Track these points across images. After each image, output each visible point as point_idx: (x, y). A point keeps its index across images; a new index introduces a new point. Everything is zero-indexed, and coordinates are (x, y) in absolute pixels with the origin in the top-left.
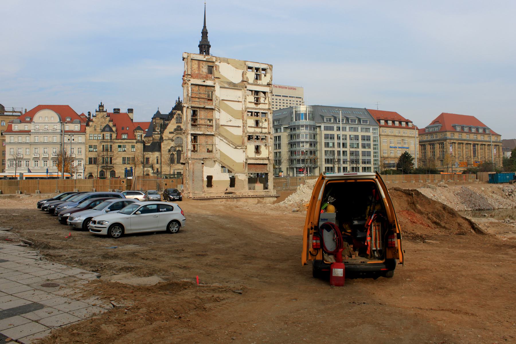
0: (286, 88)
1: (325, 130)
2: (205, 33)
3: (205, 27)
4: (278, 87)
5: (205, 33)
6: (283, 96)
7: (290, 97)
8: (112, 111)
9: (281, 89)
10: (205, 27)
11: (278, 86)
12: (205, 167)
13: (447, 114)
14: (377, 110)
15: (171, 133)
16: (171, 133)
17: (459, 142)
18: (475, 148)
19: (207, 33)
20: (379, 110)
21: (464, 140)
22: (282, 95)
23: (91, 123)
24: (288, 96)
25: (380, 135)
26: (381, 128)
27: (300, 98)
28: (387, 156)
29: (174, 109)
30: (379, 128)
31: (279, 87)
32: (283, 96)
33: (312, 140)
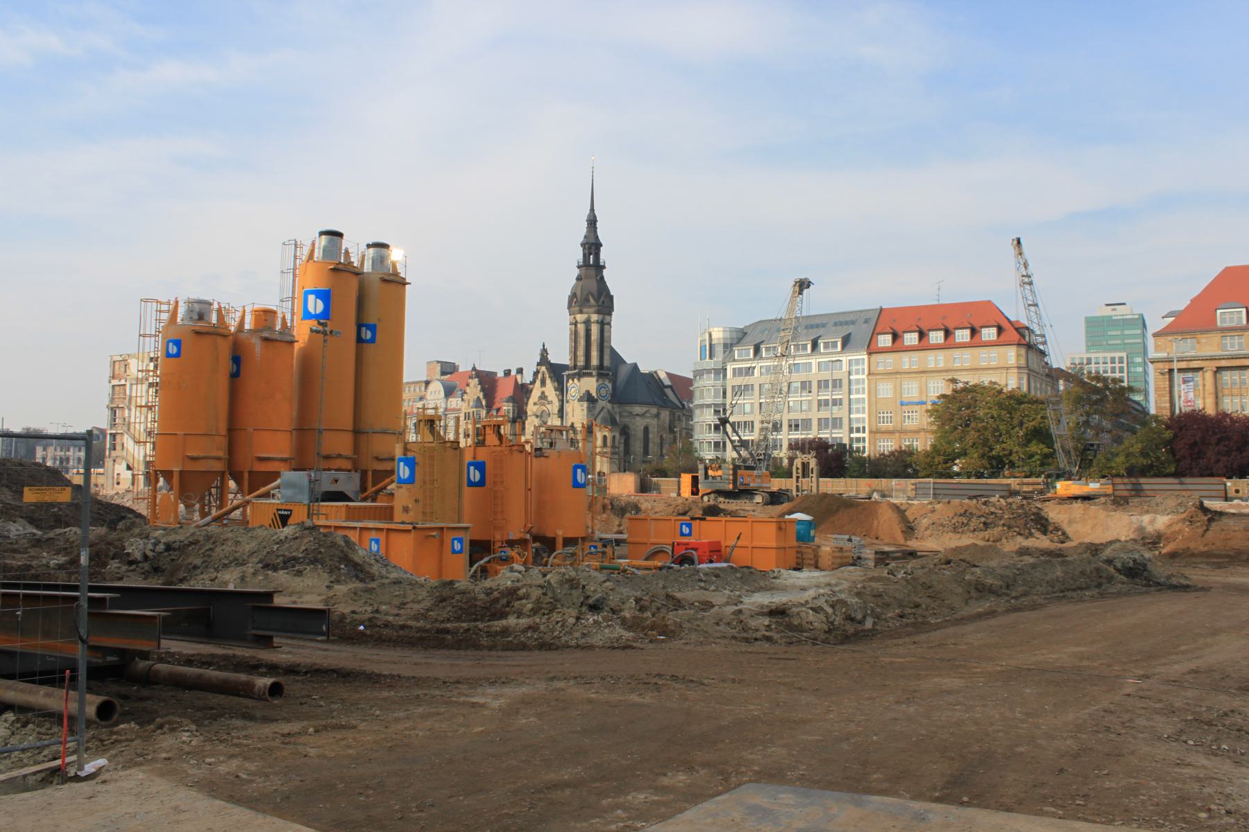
1: (734, 375)
2: (592, 222)
3: (592, 209)
5: (592, 222)
8: (503, 375)
10: (592, 209)
12: (116, 466)
14: (936, 303)
15: (535, 404)
16: (535, 404)
17: (1224, 363)
19: (596, 221)
20: (942, 302)
21: (1212, 359)
23: (465, 397)
25: (869, 374)
26: (874, 357)
28: (891, 429)
29: (538, 364)
30: (866, 357)
33: (720, 401)
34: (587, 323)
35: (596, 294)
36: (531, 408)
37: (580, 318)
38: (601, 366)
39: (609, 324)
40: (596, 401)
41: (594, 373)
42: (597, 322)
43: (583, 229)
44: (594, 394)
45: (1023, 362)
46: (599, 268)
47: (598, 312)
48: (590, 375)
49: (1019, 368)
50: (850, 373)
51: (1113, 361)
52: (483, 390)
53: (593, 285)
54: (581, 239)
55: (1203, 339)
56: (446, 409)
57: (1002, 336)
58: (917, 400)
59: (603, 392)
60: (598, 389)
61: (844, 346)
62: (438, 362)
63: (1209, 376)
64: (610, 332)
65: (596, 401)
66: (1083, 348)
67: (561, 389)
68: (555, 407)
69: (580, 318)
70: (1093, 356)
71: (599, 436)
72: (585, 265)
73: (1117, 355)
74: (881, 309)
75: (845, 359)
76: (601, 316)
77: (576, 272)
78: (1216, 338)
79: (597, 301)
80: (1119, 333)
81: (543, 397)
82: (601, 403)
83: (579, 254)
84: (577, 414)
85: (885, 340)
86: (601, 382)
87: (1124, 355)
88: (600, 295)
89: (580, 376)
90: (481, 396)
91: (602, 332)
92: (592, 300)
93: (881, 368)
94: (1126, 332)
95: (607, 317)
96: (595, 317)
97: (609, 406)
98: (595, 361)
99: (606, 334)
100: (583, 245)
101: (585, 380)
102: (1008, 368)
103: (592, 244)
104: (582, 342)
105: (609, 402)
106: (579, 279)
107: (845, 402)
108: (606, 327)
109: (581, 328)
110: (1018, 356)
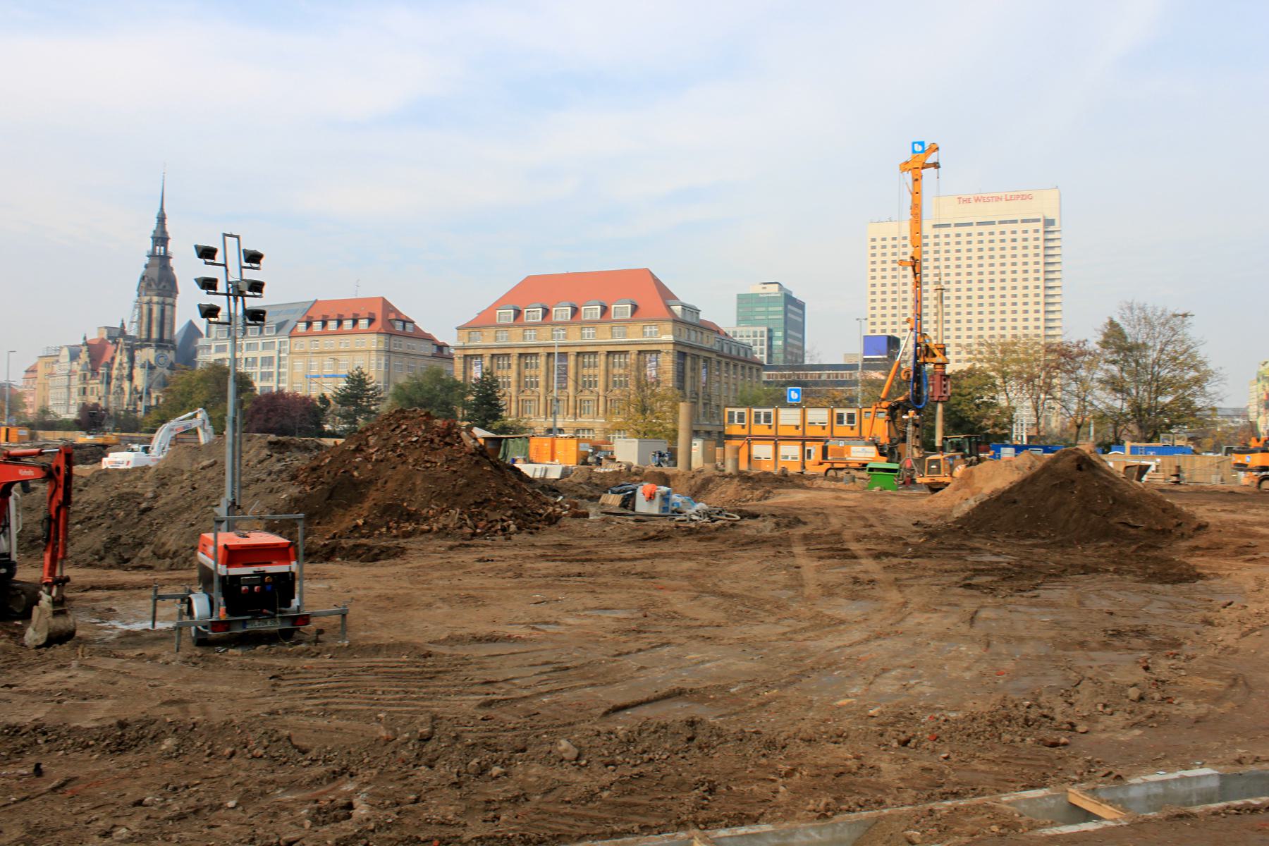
0: (998, 199)
2: (162, 219)
3: (162, 209)
4: (972, 200)
5: (162, 219)
6: (979, 224)
7: (1001, 222)
9: (981, 205)
10: (162, 209)
11: (971, 196)
13: (568, 274)
14: (354, 297)
17: (495, 352)
18: (566, 366)
22: (974, 221)
24: (997, 219)
26: (294, 340)
27: (1038, 220)
31: (977, 200)
32: (979, 224)
34: (149, 303)
35: (156, 280)
36: (115, 373)
37: (146, 299)
38: (161, 339)
39: (173, 306)
40: (155, 368)
41: (153, 344)
42: (158, 303)
43: (153, 224)
44: (153, 362)
45: (381, 347)
46: (165, 258)
47: (158, 295)
48: (150, 346)
49: (377, 351)
50: (280, 352)
51: (755, 336)
52: (89, 356)
53: (155, 273)
54: (151, 234)
55: (486, 332)
56: (70, 371)
57: (373, 325)
58: (331, 373)
59: (162, 360)
60: (157, 359)
61: (278, 331)
62: (106, 327)
63: (603, 358)
64: (173, 312)
65: (155, 368)
66: (734, 323)
67: (132, 359)
68: (126, 372)
69: (146, 299)
70: (738, 329)
71: (154, 395)
72: (152, 255)
73: (759, 329)
74: (316, 301)
75: (277, 341)
76: (161, 298)
77: (147, 260)
78: (492, 332)
79: (158, 285)
80: (763, 309)
81: (121, 364)
82: (159, 370)
83: (148, 245)
84: (140, 379)
85: (302, 327)
86: (159, 352)
87: (765, 329)
88: (161, 280)
89: (141, 347)
90: (88, 360)
91: (163, 312)
92: (154, 286)
93: (297, 349)
94: (770, 309)
95: (169, 300)
96: (155, 299)
97: (167, 372)
98: (155, 335)
99: (168, 313)
100: (153, 238)
101: (146, 350)
102: (370, 351)
103: (158, 238)
104: (145, 319)
105: (168, 368)
106: (146, 266)
107: (276, 374)
108: (168, 308)
109: (145, 307)
110: (378, 342)
